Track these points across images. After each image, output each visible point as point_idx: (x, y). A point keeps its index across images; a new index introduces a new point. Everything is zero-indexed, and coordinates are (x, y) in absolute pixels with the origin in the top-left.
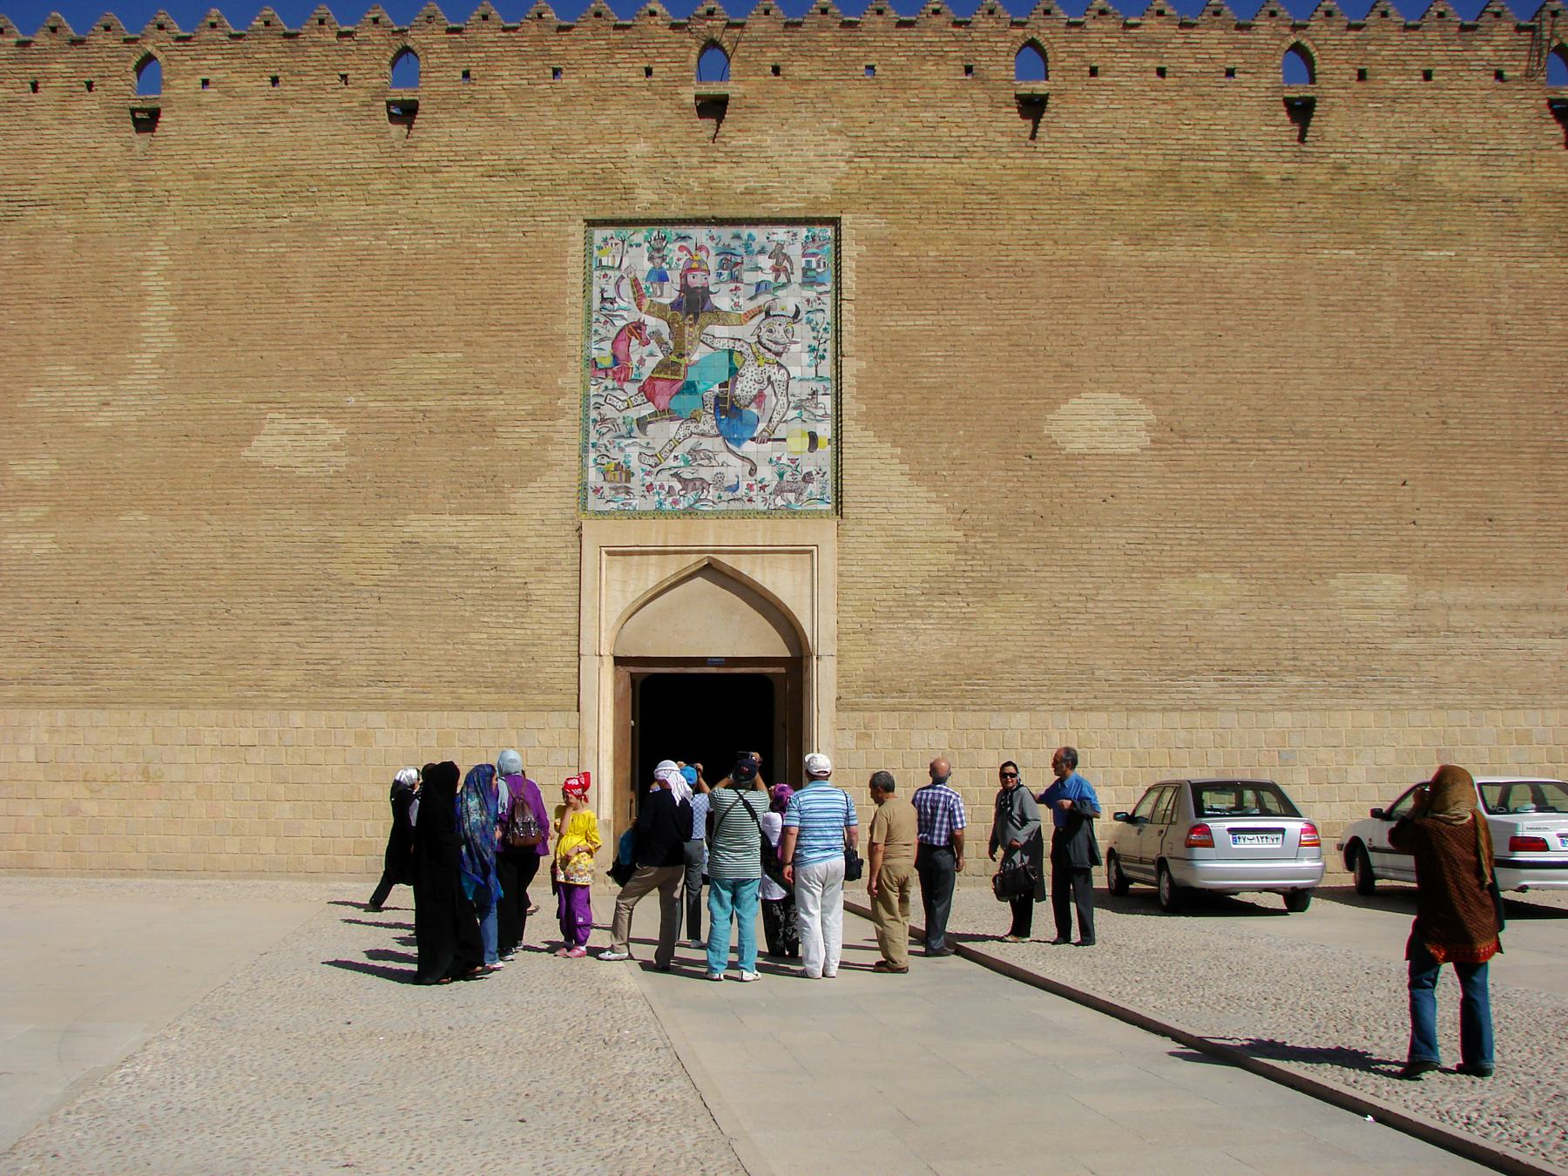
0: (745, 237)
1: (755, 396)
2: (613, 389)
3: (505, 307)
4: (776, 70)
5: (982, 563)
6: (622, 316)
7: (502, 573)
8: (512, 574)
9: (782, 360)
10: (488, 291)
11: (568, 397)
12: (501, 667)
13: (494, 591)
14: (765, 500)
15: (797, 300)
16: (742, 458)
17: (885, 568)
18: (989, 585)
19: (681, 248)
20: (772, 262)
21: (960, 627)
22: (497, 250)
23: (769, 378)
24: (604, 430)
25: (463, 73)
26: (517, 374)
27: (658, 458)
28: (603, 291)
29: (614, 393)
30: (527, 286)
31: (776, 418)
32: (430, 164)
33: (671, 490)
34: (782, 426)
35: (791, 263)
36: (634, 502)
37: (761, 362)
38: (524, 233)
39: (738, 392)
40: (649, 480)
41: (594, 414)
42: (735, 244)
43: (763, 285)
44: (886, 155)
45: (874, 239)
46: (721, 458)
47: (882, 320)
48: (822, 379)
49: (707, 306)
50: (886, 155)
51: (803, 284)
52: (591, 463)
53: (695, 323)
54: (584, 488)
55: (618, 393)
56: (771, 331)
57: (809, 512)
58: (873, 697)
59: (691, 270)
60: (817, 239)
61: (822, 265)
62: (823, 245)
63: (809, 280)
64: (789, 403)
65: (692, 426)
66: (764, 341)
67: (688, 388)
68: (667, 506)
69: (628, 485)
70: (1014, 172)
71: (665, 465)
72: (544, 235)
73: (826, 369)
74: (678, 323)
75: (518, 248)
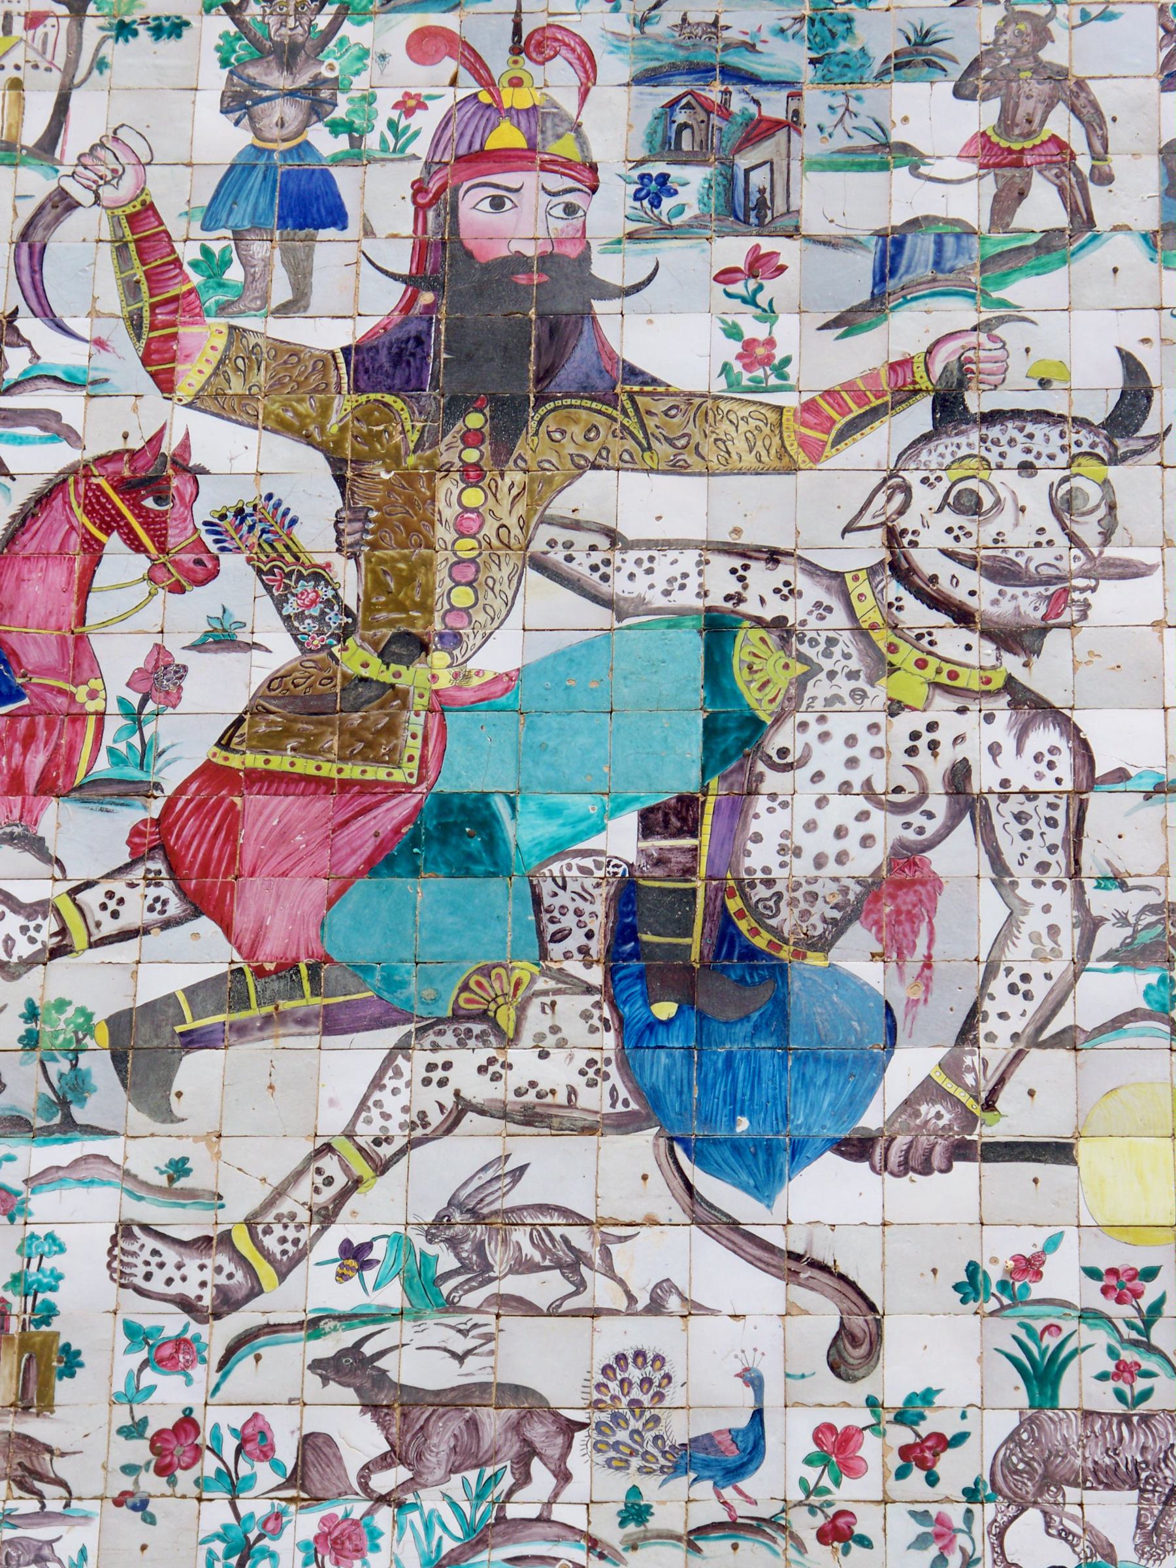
1: (873, 889)
23: (959, 775)
43: (921, 247)
64: (1089, 926)
66: (927, 561)
69: (34, 1427)
74: (394, 458)
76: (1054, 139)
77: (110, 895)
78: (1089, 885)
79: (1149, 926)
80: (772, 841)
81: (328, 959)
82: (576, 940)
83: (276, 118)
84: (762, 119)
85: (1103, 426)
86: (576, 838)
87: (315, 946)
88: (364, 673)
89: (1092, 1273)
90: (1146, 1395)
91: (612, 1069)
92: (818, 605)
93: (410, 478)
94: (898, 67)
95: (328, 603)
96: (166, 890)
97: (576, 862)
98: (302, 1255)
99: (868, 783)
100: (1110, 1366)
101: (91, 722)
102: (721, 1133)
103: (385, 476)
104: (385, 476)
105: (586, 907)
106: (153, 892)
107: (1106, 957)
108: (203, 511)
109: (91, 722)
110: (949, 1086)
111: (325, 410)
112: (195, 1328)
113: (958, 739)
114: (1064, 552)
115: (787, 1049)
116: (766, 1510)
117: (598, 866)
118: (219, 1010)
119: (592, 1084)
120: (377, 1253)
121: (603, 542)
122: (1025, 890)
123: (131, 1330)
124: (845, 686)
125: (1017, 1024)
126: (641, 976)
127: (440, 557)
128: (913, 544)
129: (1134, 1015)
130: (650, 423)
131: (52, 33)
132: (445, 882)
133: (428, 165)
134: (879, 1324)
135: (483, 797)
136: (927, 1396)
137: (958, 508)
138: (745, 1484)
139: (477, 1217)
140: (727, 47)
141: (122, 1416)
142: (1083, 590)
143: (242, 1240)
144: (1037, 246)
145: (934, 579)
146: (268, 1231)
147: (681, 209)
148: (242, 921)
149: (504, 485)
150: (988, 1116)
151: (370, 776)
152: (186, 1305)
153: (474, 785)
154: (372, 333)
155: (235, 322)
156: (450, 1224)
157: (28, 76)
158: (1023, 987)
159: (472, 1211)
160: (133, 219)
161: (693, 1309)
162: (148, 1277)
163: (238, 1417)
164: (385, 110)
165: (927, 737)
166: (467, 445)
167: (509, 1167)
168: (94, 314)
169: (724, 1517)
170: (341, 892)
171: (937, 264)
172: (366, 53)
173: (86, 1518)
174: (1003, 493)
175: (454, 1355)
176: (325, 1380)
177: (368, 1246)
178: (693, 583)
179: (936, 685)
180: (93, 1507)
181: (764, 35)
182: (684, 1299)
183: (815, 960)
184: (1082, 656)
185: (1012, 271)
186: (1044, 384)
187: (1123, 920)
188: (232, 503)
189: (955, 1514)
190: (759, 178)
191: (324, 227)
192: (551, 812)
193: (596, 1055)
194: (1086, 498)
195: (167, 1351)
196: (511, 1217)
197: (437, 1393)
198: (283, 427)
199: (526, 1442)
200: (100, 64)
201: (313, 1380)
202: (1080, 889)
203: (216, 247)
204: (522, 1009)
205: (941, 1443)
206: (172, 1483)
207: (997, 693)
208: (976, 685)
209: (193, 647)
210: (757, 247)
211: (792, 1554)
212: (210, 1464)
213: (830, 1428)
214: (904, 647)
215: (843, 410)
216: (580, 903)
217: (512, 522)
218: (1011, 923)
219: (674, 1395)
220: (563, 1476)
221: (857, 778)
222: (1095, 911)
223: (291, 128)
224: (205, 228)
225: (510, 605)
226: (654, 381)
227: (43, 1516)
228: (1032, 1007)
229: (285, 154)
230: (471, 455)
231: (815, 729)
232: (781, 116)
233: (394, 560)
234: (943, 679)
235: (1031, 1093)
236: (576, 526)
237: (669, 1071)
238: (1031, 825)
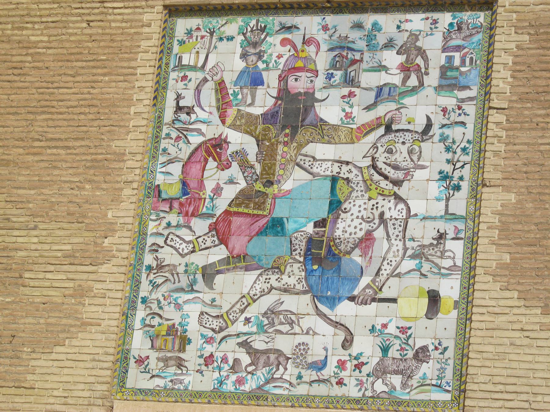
0: (368, 26)
1: (361, 240)
2: (178, 226)
3: (55, 117)
6: (199, 132)
9: (402, 192)
10: (36, 96)
11: (118, 234)
14: (361, 383)
15: (430, 110)
16: (337, 324)
19: (284, 42)
20: (402, 59)
22: (52, 45)
23: (382, 214)
24: (160, 280)
26: (58, 203)
28: (179, 97)
30: (86, 90)
31: (387, 269)
34: (393, 281)
35: (426, 59)
36: (187, 379)
37: (374, 193)
38: (89, 22)
39: (338, 233)
40: (209, 349)
41: (149, 259)
42: (355, 35)
43: (386, 90)
45: (542, 25)
46: (306, 323)
47: (542, 137)
48: (454, 217)
51: (439, 88)
52: (138, 324)
55: (184, 232)
56: (390, 151)
60: (464, 27)
61: (468, 61)
62: (471, 35)
63: (448, 82)
64: (406, 249)
65: (274, 277)
66: (380, 165)
67: (273, 225)
68: (229, 386)
69: (182, 355)
71: (232, 330)
72: (113, 25)
74: (269, 140)
75: (80, 42)
76: (417, 64)
77: (204, 239)
78: (407, 240)
79: (418, 250)
80: (341, 229)
81: (247, 255)
82: (298, 251)
83: (251, 60)
84: (355, 59)
85: (421, 133)
86: (300, 228)
87: (245, 251)
88: (260, 189)
89: (398, 328)
90: (406, 355)
91: (303, 280)
92: (356, 175)
93: (272, 144)
94: (385, 47)
95: (253, 173)
96: (215, 239)
97: (300, 233)
98: (237, 320)
99: (362, 216)
100: (399, 348)
101: (203, 200)
102: (325, 295)
103: (267, 144)
104: (267, 144)
105: (301, 244)
106: (213, 239)
107: (408, 257)
108: (229, 152)
109: (203, 200)
110: (372, 285)
111: (256, 128)
112: (215, 335)
113: (383, 206)
114: (409, 163)
115: (340, 276)
116: (326, 378)
117: (304, 234)
118: (224, 265)
119: (299, 283)
120: (252, 320)
121: (312, 160)
122: (393, 241)
123: (202, 335)
124: (360, 194)
125: (388, 272)
126: (311, 259)
127: (277, 163)
128: (377, 161)
129: (414, 270)
130: (324, 132)
131: (206, 40)
132: (272, 237)
133: (282, 71)
134: (353, 338)
135: (282, 218)
136: (361, 354)
137: (388, 152)
138: (322, 372)
139: (273, 313)
140: (349, 42)
142: (412, 172)
143: (225, 316)
144: (411, 90)
145: (381, 169)
146: (230, 314)
147: (335, 81)
148: (230, 246)
149: (292, 146)
150: (380, 292)
151: (259, 213)
152: (213, 330)
153: (280, 216)
154: (267, 111)
155: (239, 108)
156: (267, 314)
157: (200, 50)
158: (390, 263)
159: (272, 311)
160: (219, 84)
161: (315, 333)
162: (206, 324)
163: (222, 354)
164: (274, 58)
165: (376, 206)
166: (285, 137)
167: (281, 301)
168: (210, 106)
169: (317, 379)
170: (251, 239)
171: (389, 94)
172: (271, 44)
173: (191, 375)
174: (398, 149)
175: (266, 342)
176: (239, 347)
177: (250, 318)
178: (330, 169)
179: (379, 194)
180: (192, 372)
181: (357, 39)
182: (313, 331)
183: (347, 256)
184: (411, 187)
185: (405, 96)
186: (409, 123)
187: (413, 248)
188: (235, 150)
189: (364, 379)
190: (353, 74)
191: (259, 85)
192: (295, 222)
193: (300, 277)
194: (415, 150)
195: (209, 340)
196: (280, 313)
197: (262, 350)
198: (247, 132)
199: (279, 362)
200: (215, 47)
201: (237, 347)
202: (405, 241)
203: (236, 90)
204: (286, 267)
205: (363, 364)
206: (208, 368)
207: (392, 196)
208: (388, 194)
209: (225, 183)
210: (351, 90)
211: (331, 387)
212: (215, 364)
213: (341, 360)
214: (373, 185)
215: (366, 129)
216: (300, 243)
217: (293, 155)
218: (389, 248)
219: (310, 352)
220: (286, 369)
222: (407, 246)
223: (254, 62)
224: (234, 86)
225: (291, 174)
226: (326, 122)
227: (182, 374)
228: (392, 268)
229: (252, 68)
230: (286, 139)
231: (353, 203)
232: (359, 59)
233: (268, 163)
234: (381, 192)
235: (390, 287)
236: (306, 156)
237: (315, 281)
238: (396, 226)
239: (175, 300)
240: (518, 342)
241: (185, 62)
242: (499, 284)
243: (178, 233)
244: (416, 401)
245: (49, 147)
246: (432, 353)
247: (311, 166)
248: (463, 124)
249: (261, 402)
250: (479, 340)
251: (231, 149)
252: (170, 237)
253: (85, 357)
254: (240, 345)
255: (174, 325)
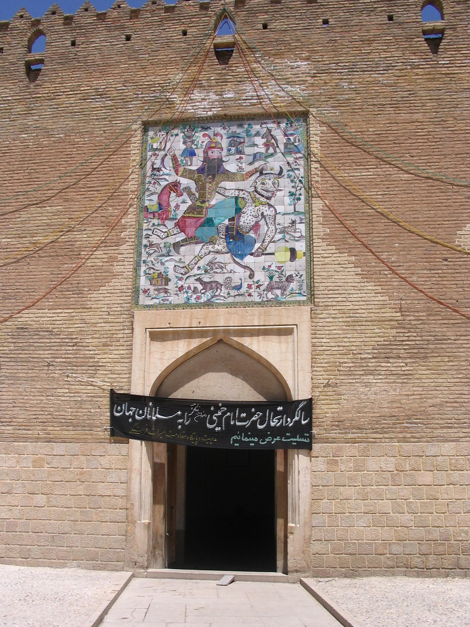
1: (253, 226)
2: (158, 225)
4: (265, 26)
5: (415, 334)
7: (80, 348)
8: (87, 348)
9: (272, 202)
12: (77, 412)
13: (74, 360)
14: (260, 295)
15: (281, 164)
16: (245, 267)
17: (346, 340)
18: (422, 351)
19: (204, 135)
20: (264, 140)
21: (401, 381)
23: (262, 213)
24: (152, 252)
25: (72, 41)
27: (188, 268)
28: (153, 164)
29: (159, 228)
31: (268, 240)
32: (49, 95)
33: (195, 290)
34: (272, 245)
35: (276, 141)
36: (170, 299)
37: (257, 204)
39: (241, 223)
40: (180, 283)
41: (145, 242)
44: (338, 71)
48: (299, 213)
49: (220, 171)
50: (338, 71)
52: (142, 273)
53: (213, 180)
54: (136, 291)
56: (263, 184)
57: (290, 302)
58: (339, 433)
59: (211, 148)
61: (297, 140)
62: (297, 128)
64: (276, 229)
65: (210, 247)
66: (259, 190)
67: (208, 222)
68: (193, 301)
69: (166, 287)
70: (424, 77)
71: (191, 273)
73: (301, 206)
74: (201, 181)
80: (243, 221)
93: (203, 183)
122: (269, 226)
123: (176, 277)
124: (250, 204)
141: (175, 286)
143: (187, 267)
148: (186, 233)
152: (182, 274)
161: (235, 272)
163: (187, 285)
164: (200, 143)
183: (247, 234)
190: (240, 148)
196: (215, 263)
198: (190, 178)
200: (170, 139)
205: (261, 285)
212: (185, 290)
219: (233, 281)
220: (221, 290)
221: (251, 214)
227: (168, 296)
239: (161, 260)
240: (338, 270)
241: (155, 147)
242: (325, 243)
243: (159, 228)
244: (289, 301)
245: (89, 191)
246: (295, 278)
247: (224, 192)
248: (298, 169)
249: (210, 307)
250: (319, 270)
251: (182, 187)
252: (155, 230)
253: (117, 291)
254: (196, 280)
255: (161, 273)
